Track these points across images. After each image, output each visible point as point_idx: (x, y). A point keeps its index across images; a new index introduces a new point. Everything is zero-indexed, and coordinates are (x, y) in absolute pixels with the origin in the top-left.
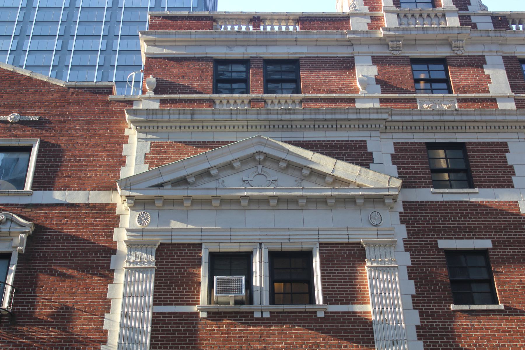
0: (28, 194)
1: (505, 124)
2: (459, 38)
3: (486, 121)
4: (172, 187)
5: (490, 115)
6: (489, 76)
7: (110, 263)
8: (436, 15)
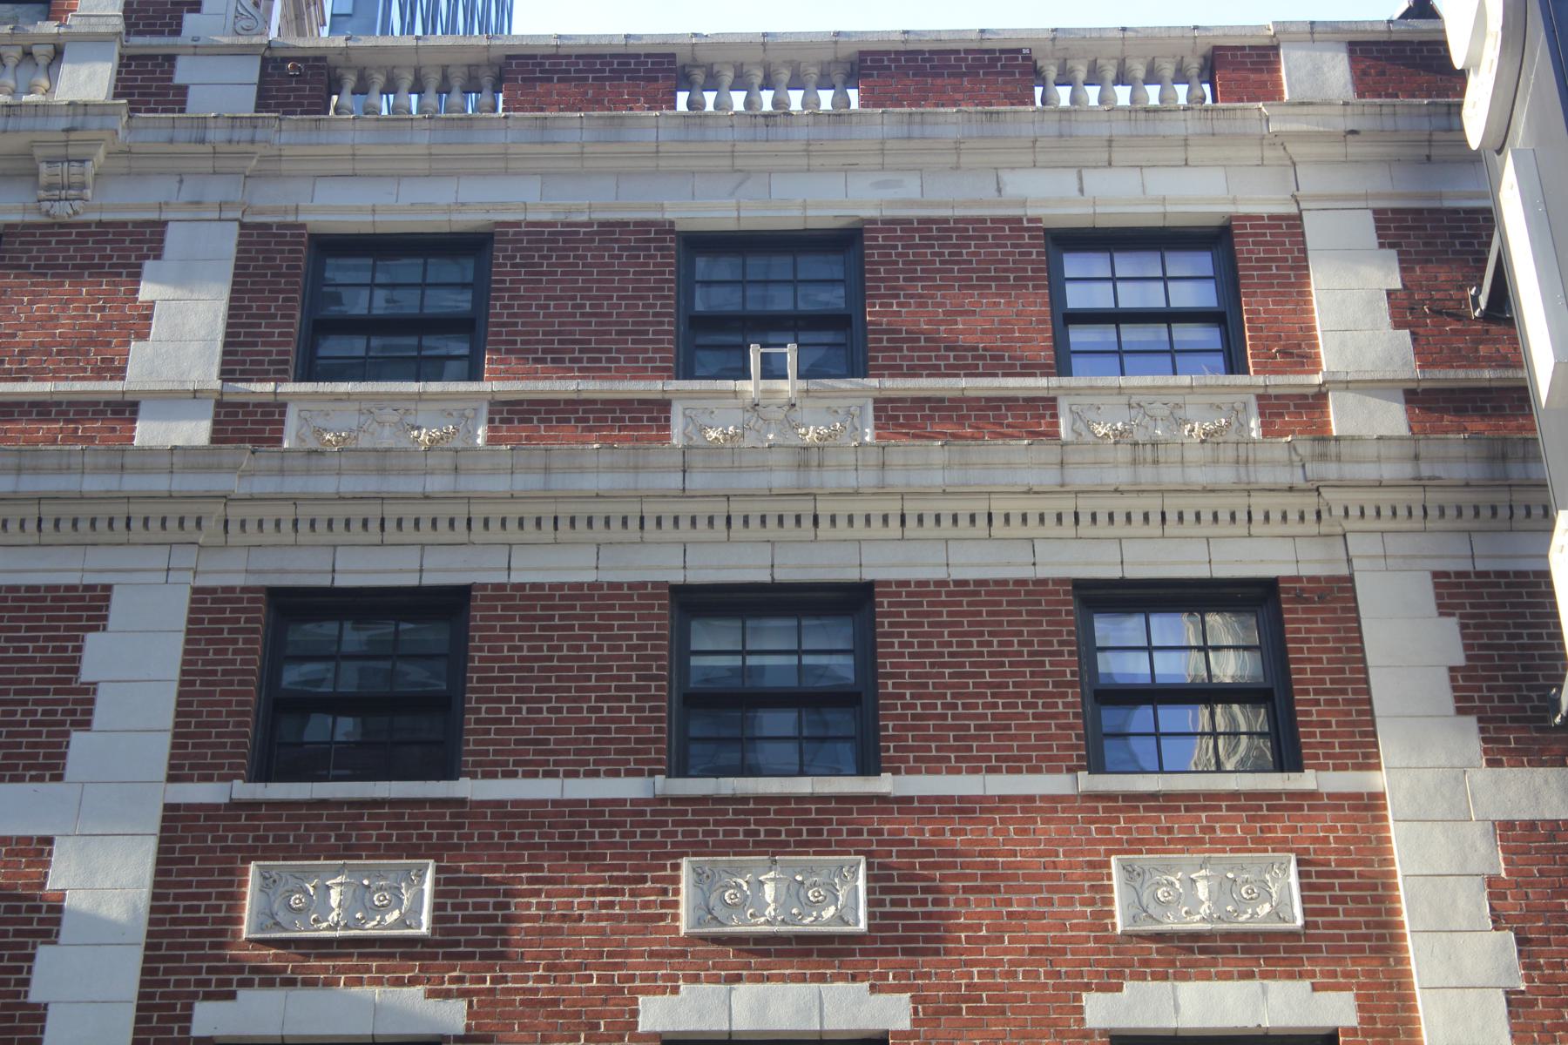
1: (119, 510)
2: (72, 151)
3: (39, 499)
5: (59, 470)
6: (151, 306)
8: (28, 54)
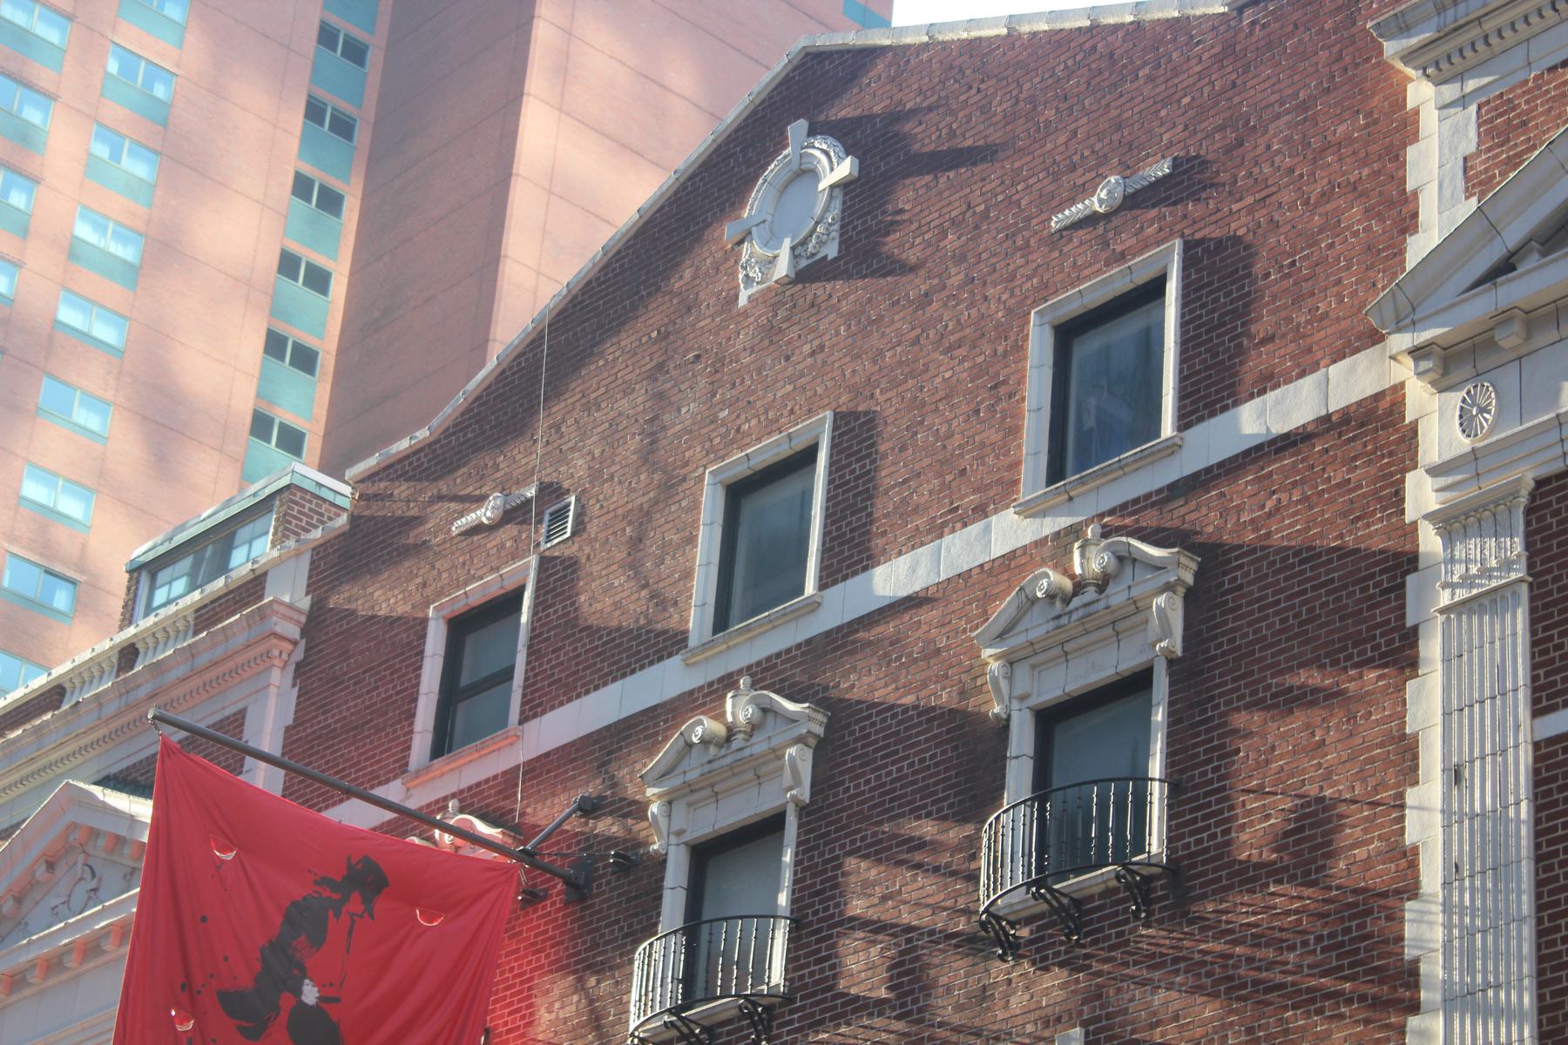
0: (1172, 448)
4: (1544, 255)
7: (1403, 606)
